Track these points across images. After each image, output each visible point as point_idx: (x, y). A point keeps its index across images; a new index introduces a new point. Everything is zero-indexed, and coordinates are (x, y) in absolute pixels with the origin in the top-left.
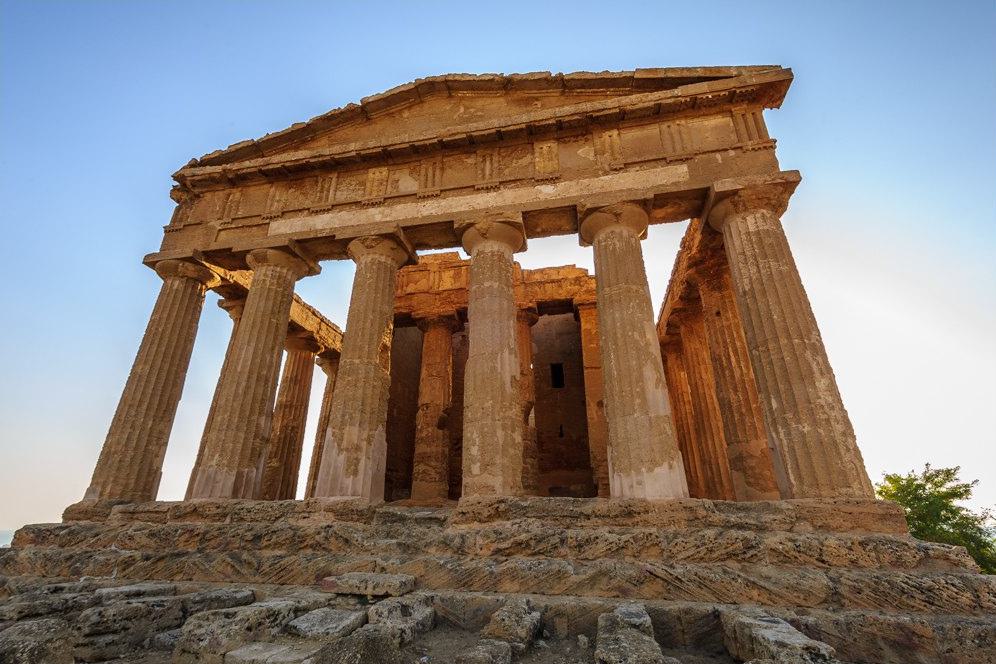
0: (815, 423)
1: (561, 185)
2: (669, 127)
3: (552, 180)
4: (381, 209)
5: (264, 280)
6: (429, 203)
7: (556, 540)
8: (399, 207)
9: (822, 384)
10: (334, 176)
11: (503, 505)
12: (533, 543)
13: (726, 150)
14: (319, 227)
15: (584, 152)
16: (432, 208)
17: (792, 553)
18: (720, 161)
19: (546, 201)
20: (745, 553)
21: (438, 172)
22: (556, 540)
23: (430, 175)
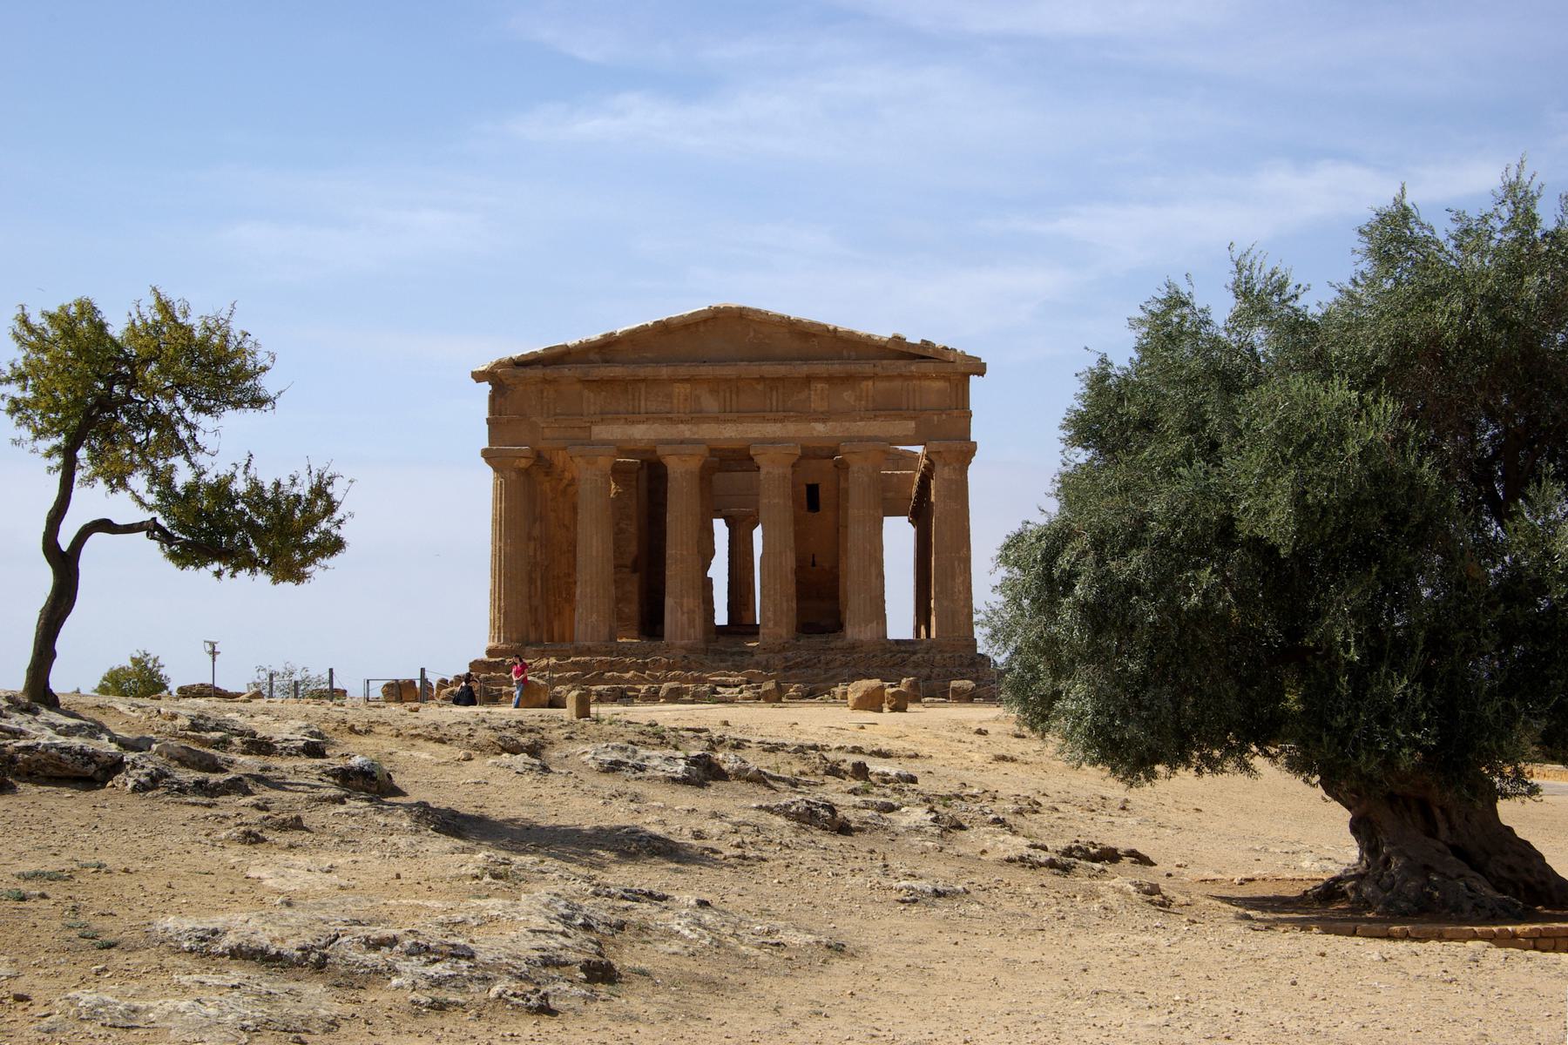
3: (824, 417)
4: (690, 426)
7: (816, 660)
8: (705, 426)
9: (959, 580)
10: (643, 386)
14: (638, 436)
15: (848, 396)
21: (734, 396)
22: (816, 660)
23: (728, 395)
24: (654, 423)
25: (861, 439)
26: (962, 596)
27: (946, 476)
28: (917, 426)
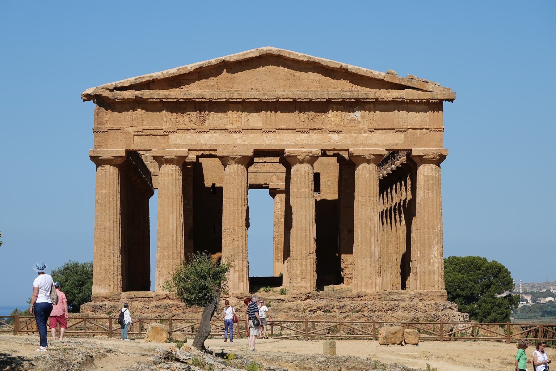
0: (429, 264)
1: (342, 135)
2: (399, 107)
5: (172, 174)
6: (270, 135)
11: (311, 294)
12: (324, 307)
13: (423, 129)
16: (272, 140)
17: (408, 308)
18: (419, 135)
19: (334, 144)
20: (394, 308)
24: (215, 133)
25: (364, 145)
26: (436, 260)
27: (426, 174)
28: (405, 137)
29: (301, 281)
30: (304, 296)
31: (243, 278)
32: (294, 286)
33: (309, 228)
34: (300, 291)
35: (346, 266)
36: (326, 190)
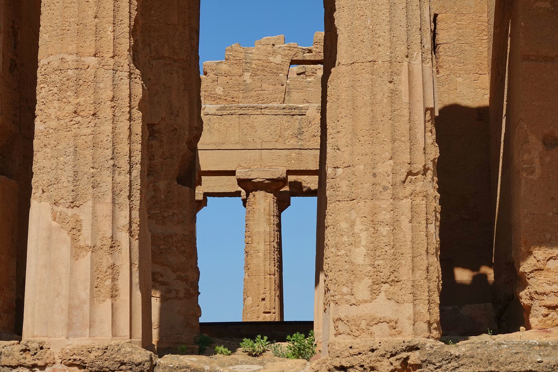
11: (417, 353)
29: (374, 293)
30: (386, 362)
31: (114, 279)
32: (342, 316)
33: (406, 64)
34: (369, 338)
35: (539, 265)
36: (454, 63)
